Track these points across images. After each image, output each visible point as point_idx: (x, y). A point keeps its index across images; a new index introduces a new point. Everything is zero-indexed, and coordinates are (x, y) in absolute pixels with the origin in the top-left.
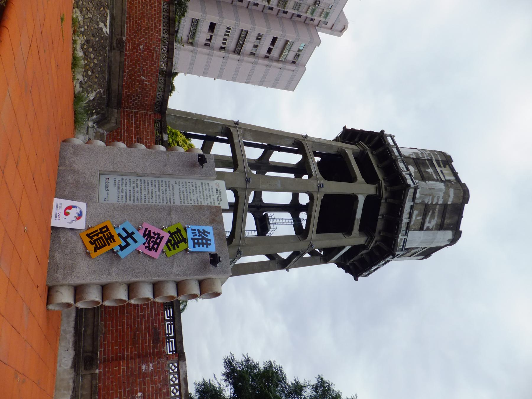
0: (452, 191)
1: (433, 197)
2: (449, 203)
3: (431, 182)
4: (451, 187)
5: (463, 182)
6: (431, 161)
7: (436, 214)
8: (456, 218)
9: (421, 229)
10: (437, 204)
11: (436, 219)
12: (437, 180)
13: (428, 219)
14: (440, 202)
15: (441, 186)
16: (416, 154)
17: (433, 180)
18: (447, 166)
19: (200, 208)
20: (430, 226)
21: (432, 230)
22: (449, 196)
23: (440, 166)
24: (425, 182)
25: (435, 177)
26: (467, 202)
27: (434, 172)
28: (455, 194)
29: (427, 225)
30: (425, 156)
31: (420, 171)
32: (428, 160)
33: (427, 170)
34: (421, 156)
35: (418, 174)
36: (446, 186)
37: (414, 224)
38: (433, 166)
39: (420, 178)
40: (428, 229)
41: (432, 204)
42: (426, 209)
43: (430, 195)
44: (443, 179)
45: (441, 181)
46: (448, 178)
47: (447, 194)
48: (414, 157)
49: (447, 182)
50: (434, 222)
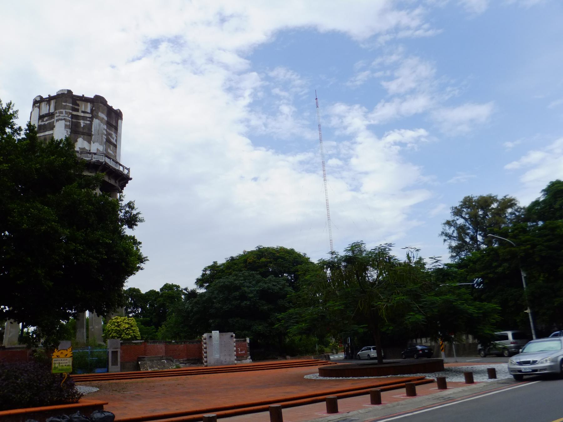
0: (101, 115)
1: (103, 134)
2: (106, 118)
3: (93, 129)
4: (98, 113)
5: (92, 96)
6: (73, 117)
7: (111, 132)
8: (113, 114)
9: (115, 146)
10: (107, 131)
11: (113, 133)
12: (91, 122)
13: (112, 140)
14: (105, 127)
15: (96, 122)
16: (66, 126)
17: (91, 125)
18: (78, 102)
19: (220, 338)
20: (115, 138)
21: (117, 137)
22: (103, 118)
23: (77, 110)
24: (93, 135)
25: (88, 122)
26: (106, 102)
27: (83, 120)
28: (103, 113)
29: (114, 141)
30: (68, 118)
31: (83, 134)
32: (72, 118)
33: (82, 126)
34: (68, 123)
35: (85, 137)
36: (97, 117)
37: (114, 152)
38: (77, 117)
39: (89, 137)
40: (116, 141)
41: (106, 135)
42: (108, 141)
43: (102, 136)
44: (90, 116)
45: (92, 119)
46: (89, 111)
47: (101, 120)
48: (69, 131)
49: (94, 114)
50: (114, 135)
